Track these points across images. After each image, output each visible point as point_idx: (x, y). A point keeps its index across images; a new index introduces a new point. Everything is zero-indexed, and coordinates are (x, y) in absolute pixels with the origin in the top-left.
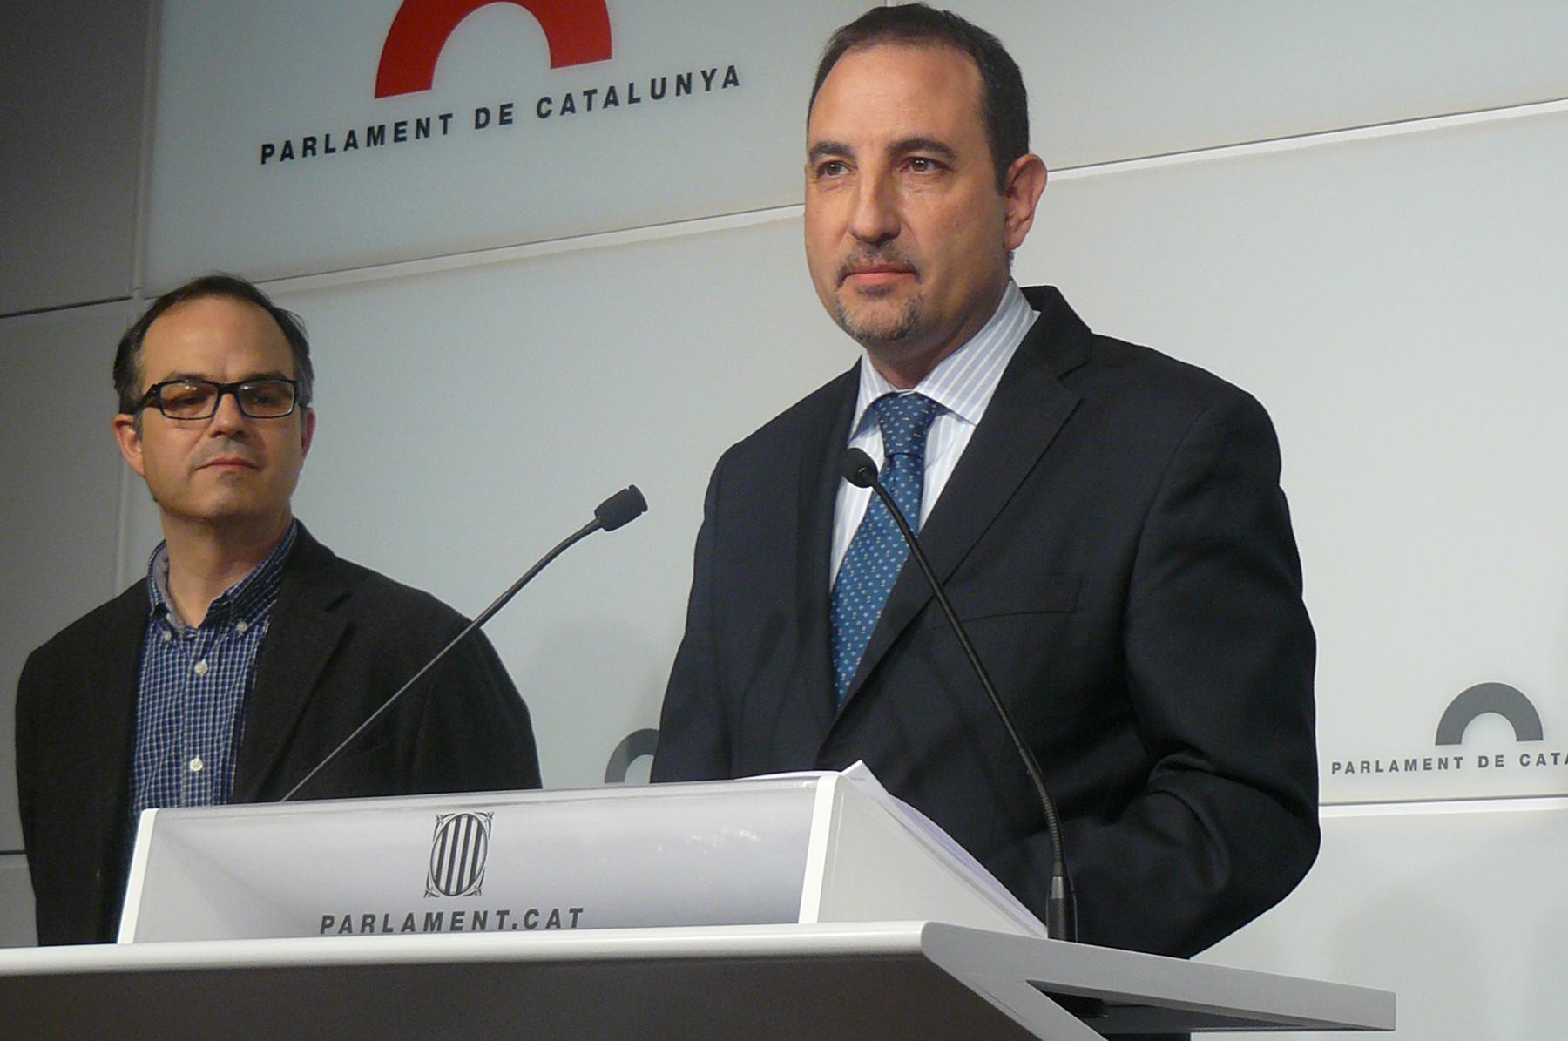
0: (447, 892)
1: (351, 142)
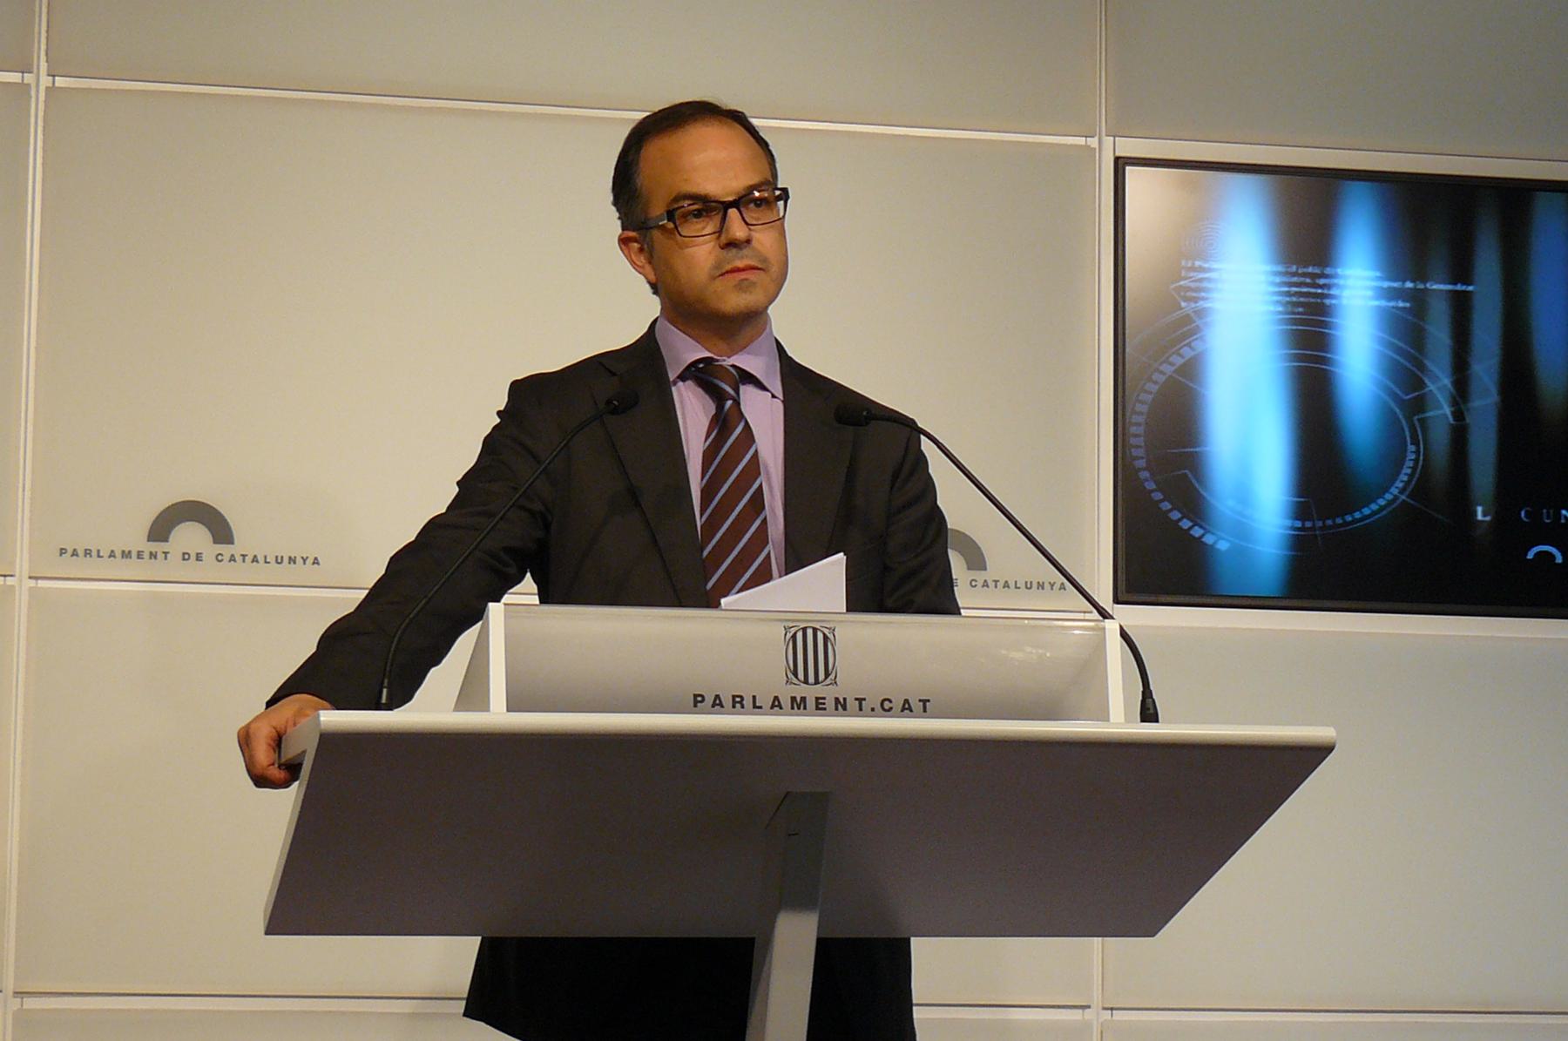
0: (806, 682)
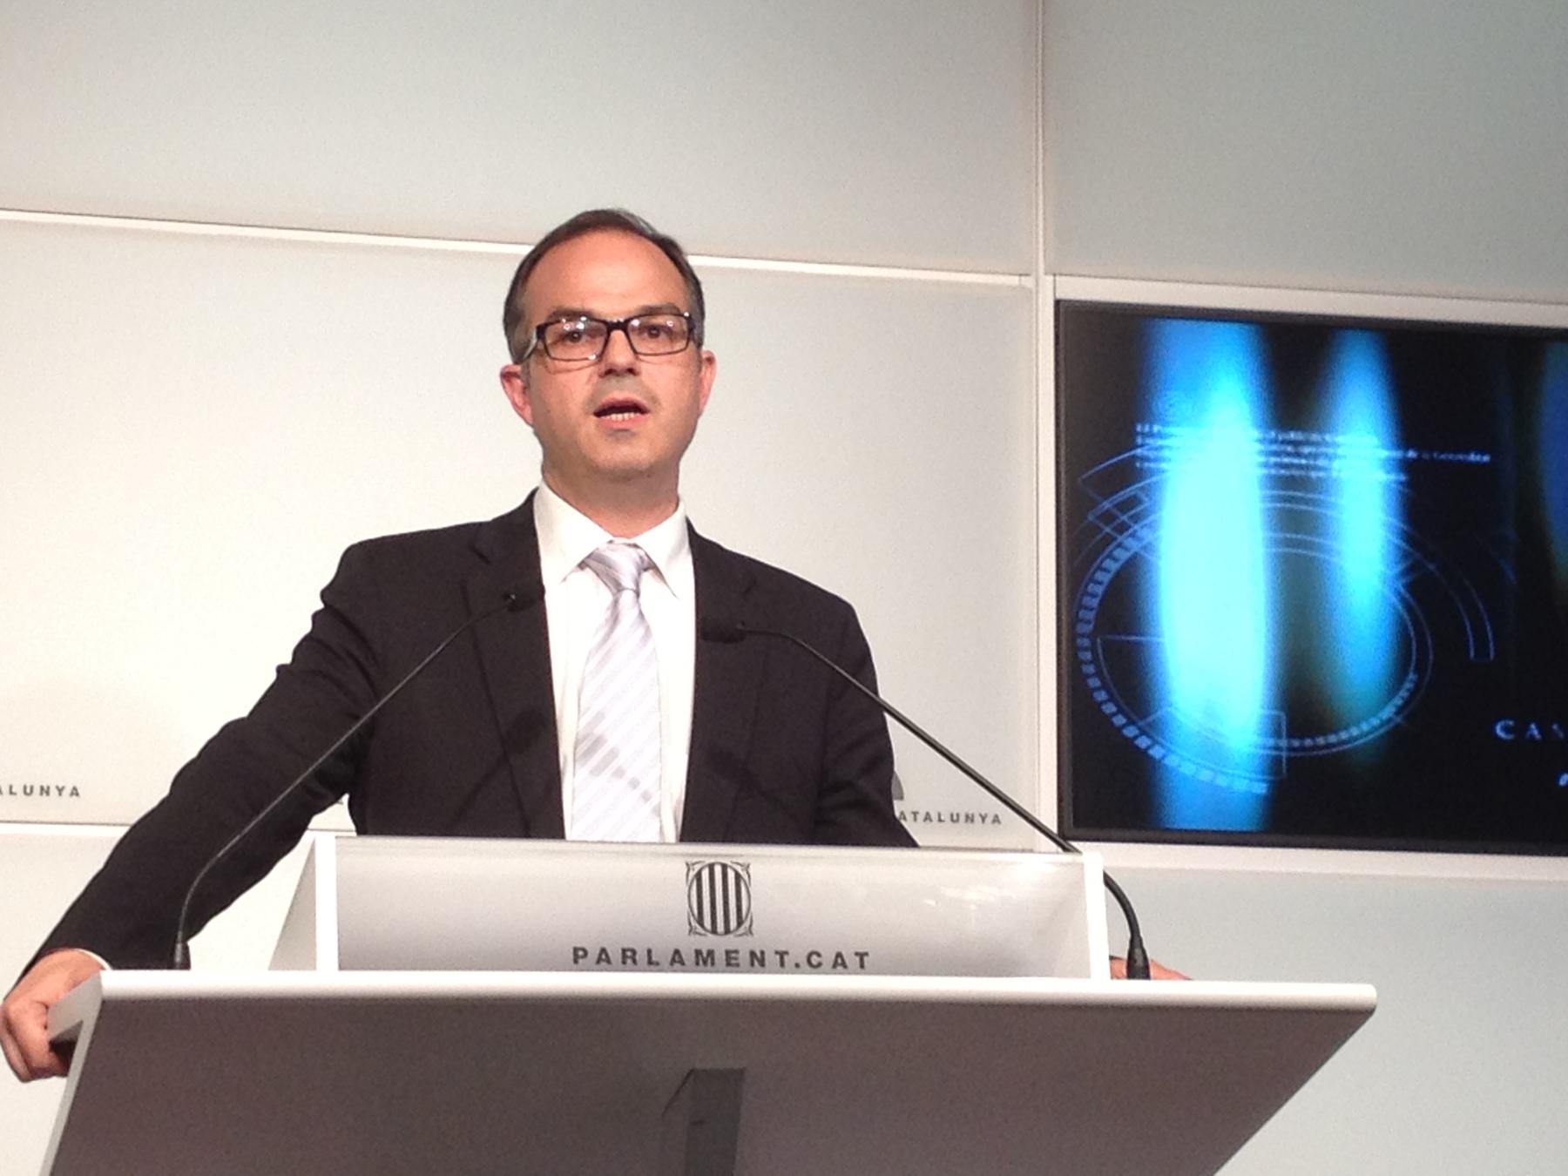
0: (714, 931)
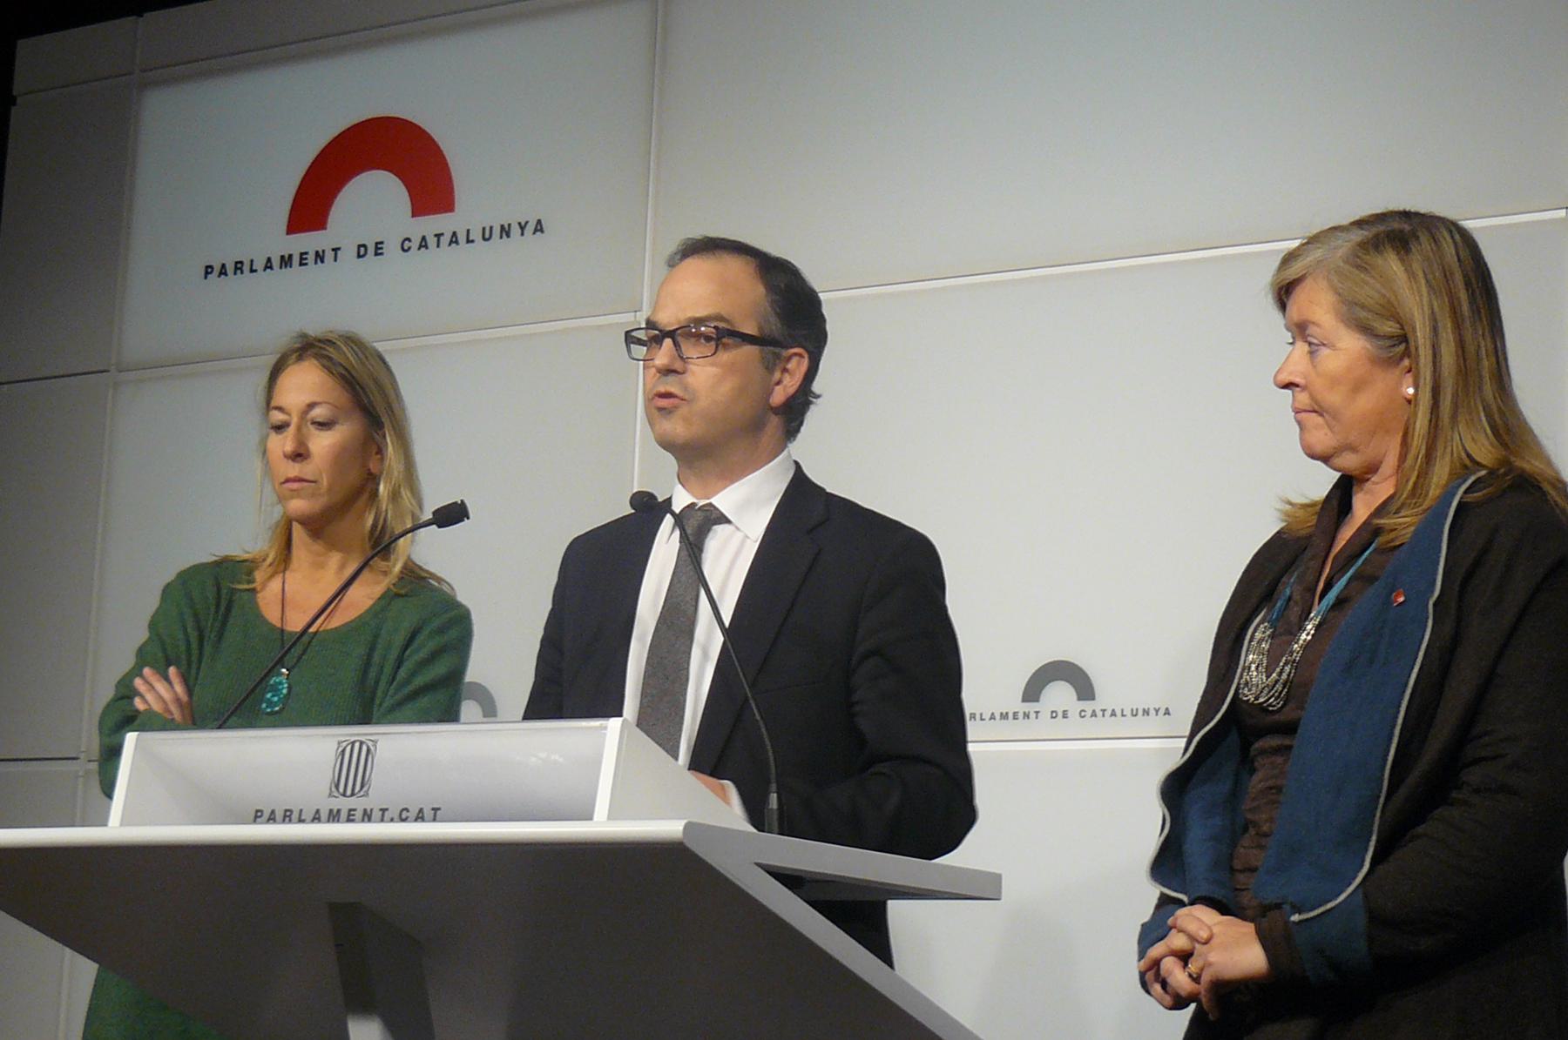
1: (268, 265)
